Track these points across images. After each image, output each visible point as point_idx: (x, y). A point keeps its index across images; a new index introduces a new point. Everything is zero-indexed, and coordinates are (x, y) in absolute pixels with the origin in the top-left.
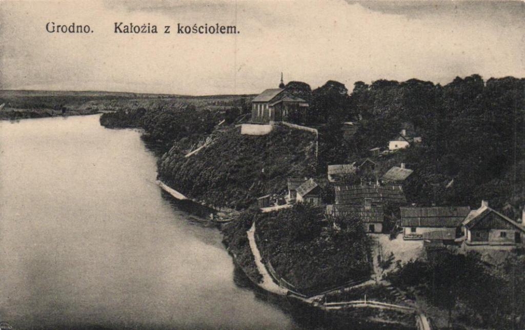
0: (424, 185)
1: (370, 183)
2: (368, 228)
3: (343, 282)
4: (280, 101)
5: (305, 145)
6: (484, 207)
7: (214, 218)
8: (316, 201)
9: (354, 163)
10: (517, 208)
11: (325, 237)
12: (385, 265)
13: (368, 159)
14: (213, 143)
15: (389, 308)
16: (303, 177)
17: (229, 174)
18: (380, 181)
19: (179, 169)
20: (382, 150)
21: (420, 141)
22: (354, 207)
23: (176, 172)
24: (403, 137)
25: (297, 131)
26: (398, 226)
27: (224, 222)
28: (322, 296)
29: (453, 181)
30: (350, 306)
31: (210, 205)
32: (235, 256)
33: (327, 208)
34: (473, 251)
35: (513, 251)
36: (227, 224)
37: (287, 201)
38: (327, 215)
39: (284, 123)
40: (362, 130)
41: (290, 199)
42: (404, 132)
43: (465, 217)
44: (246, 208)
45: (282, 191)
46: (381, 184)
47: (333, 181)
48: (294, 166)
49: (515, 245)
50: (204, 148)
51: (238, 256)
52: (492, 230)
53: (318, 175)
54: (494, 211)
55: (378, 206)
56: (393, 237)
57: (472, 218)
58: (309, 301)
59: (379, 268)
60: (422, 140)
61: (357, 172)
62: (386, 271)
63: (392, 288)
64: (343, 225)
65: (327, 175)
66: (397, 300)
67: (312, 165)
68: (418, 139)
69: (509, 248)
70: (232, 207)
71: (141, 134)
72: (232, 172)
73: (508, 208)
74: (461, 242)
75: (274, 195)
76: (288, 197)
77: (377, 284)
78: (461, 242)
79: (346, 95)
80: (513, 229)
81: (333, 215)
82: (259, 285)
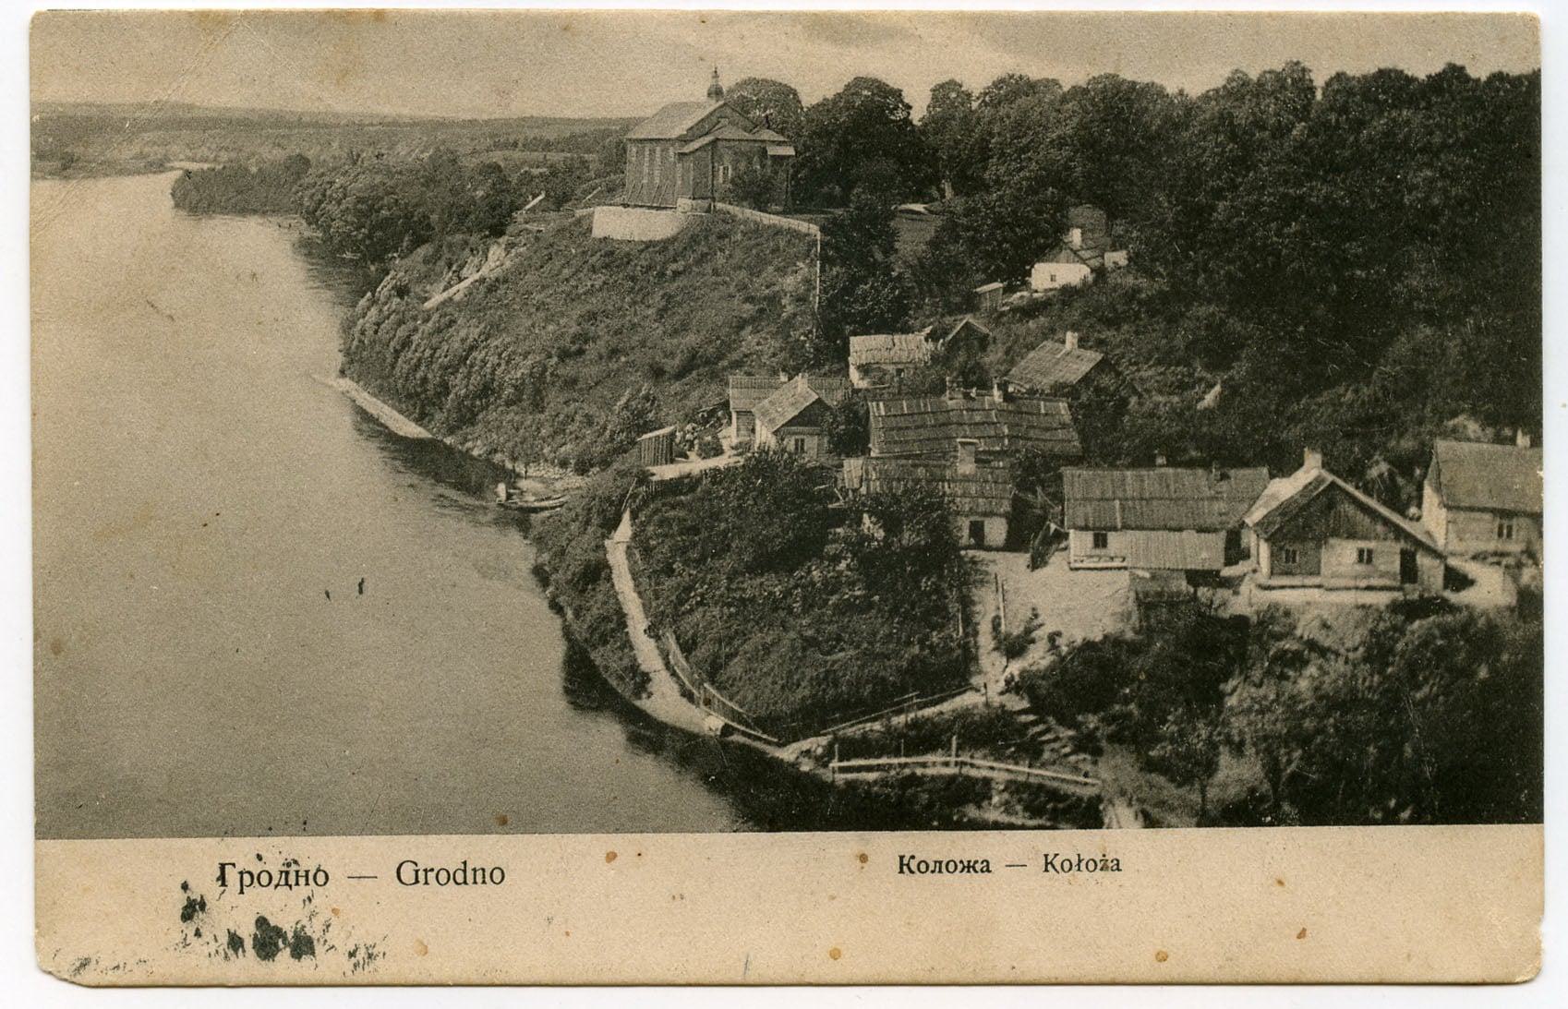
0: (1134, 400)
1: (973, 392)
2: (966, 532)
3: (883, 698)
4: (709, 138)
5: (782, 271)
6: (1311, 469)
7: (509, 496)
8: (811, 443)
9: (928, 330)
10: (1407, 473)
11: (836, 559)
12: (1013, 648)
13: (969, 318)
14: (508, 264)
15: (1021, 778)
16: (775, 373)
17: (555, 359)
18: (1003, 387)
19: (406, 343)
20: (1010, 290)
21: (1123, 262)
22: (926, 466)
23: (397, 353)
24: (1075, 252)
25: (758, 230)
26: (1053, 527)
27: (535, 510)
28: (824, 741)
29: (1218, 388)
30: (907, 771)
31: (498, 457)
32: (570, 614)
33: (846, 468)
34: (1274, 606)
35: (1394, 607)
36: (547, 514)
37: (725, 444)
38: (844, 491)
39: (720, 205)
40: (951, 229)
41: (735, 441)
42: (1076, 236)
43: (1254, 499)
44: (605, 464)
45: (712, 413)
46: (1008, 397)
47: (863, 384)
48: (749, 339)
49: (1400, 589)
50: (482, 280)
51: (577, 615)
52: (1332, 541)
53: (818, 365)
54: (1340, 482)
55: (994, 464)
56: (1037, 562)
57: (1274, 504)
58: (787, 754)
59: (996, 654)
60: (1130, 259)
61: (935, 358)
62: (1015, 667)
63: (1032, 718)
64: (892, 524)
65: (847, 366)
66: (1046, 755)
67: (806, 334)
68: (1120, 257)
69: (1382, 599)
70: (564, 464)
71: (296, 236)
72: (564, 355)
73: (1381, 475)
74: (1241, 578)
75: (689, 427)
76: (730, 435)
77: (987, 705)
78: (1241, 578)
79: (907, 121)
80: (1397, 539)
81: (863, 490)
82: (638, 703)
